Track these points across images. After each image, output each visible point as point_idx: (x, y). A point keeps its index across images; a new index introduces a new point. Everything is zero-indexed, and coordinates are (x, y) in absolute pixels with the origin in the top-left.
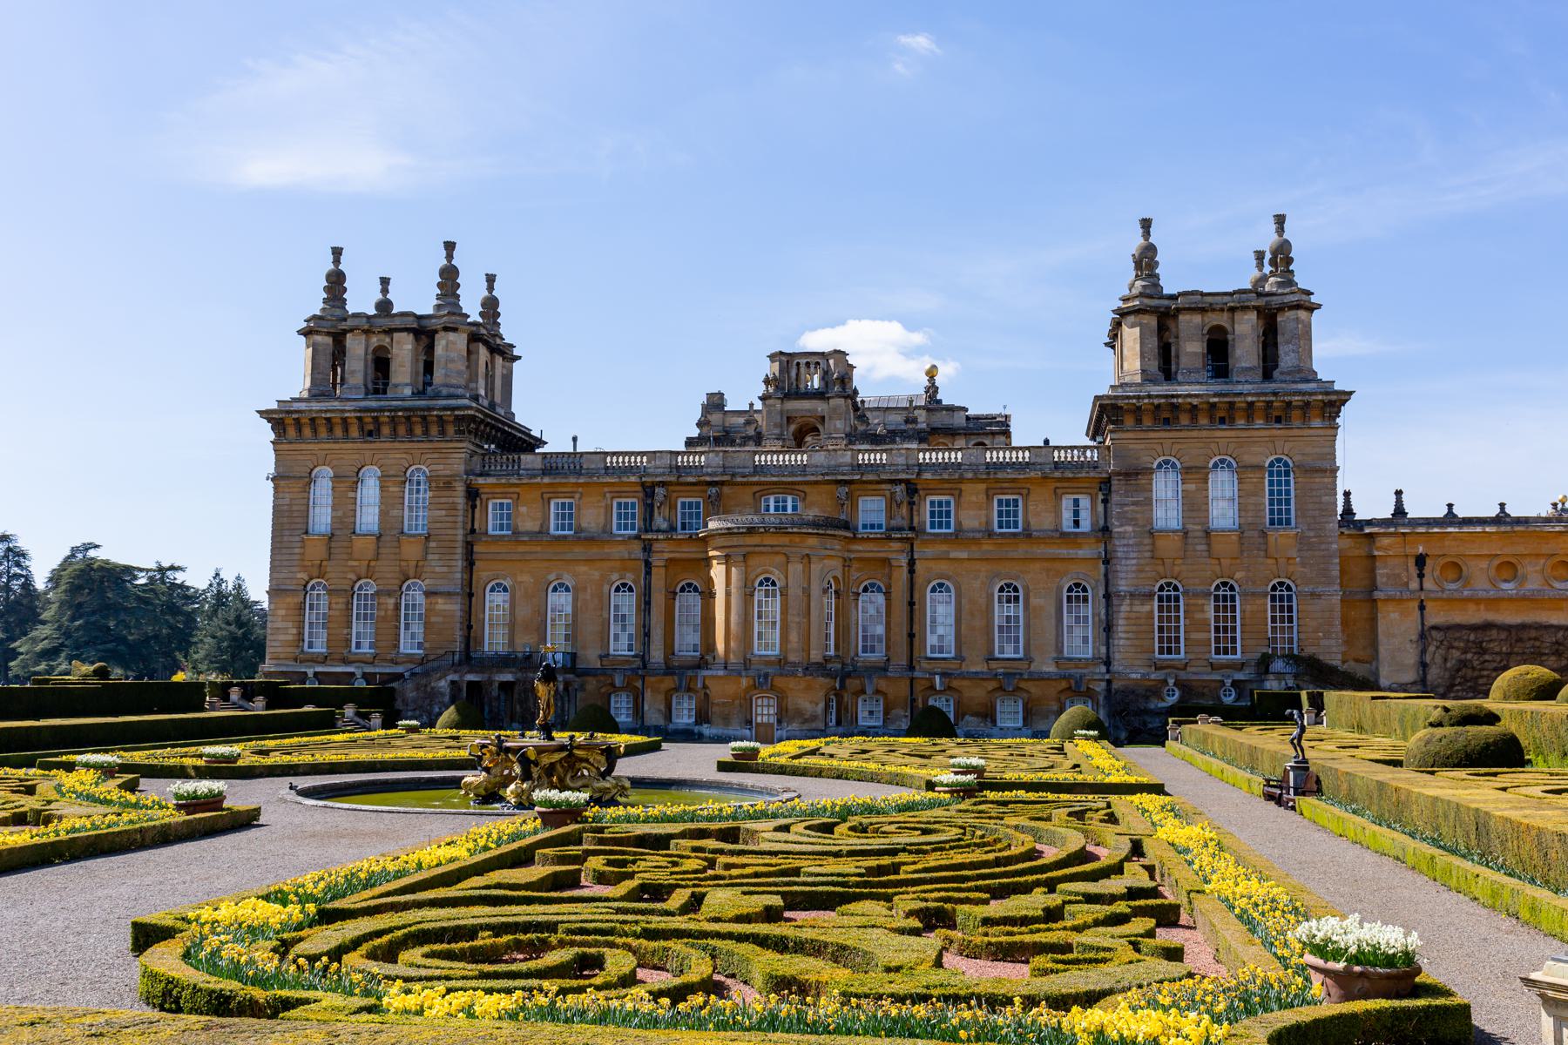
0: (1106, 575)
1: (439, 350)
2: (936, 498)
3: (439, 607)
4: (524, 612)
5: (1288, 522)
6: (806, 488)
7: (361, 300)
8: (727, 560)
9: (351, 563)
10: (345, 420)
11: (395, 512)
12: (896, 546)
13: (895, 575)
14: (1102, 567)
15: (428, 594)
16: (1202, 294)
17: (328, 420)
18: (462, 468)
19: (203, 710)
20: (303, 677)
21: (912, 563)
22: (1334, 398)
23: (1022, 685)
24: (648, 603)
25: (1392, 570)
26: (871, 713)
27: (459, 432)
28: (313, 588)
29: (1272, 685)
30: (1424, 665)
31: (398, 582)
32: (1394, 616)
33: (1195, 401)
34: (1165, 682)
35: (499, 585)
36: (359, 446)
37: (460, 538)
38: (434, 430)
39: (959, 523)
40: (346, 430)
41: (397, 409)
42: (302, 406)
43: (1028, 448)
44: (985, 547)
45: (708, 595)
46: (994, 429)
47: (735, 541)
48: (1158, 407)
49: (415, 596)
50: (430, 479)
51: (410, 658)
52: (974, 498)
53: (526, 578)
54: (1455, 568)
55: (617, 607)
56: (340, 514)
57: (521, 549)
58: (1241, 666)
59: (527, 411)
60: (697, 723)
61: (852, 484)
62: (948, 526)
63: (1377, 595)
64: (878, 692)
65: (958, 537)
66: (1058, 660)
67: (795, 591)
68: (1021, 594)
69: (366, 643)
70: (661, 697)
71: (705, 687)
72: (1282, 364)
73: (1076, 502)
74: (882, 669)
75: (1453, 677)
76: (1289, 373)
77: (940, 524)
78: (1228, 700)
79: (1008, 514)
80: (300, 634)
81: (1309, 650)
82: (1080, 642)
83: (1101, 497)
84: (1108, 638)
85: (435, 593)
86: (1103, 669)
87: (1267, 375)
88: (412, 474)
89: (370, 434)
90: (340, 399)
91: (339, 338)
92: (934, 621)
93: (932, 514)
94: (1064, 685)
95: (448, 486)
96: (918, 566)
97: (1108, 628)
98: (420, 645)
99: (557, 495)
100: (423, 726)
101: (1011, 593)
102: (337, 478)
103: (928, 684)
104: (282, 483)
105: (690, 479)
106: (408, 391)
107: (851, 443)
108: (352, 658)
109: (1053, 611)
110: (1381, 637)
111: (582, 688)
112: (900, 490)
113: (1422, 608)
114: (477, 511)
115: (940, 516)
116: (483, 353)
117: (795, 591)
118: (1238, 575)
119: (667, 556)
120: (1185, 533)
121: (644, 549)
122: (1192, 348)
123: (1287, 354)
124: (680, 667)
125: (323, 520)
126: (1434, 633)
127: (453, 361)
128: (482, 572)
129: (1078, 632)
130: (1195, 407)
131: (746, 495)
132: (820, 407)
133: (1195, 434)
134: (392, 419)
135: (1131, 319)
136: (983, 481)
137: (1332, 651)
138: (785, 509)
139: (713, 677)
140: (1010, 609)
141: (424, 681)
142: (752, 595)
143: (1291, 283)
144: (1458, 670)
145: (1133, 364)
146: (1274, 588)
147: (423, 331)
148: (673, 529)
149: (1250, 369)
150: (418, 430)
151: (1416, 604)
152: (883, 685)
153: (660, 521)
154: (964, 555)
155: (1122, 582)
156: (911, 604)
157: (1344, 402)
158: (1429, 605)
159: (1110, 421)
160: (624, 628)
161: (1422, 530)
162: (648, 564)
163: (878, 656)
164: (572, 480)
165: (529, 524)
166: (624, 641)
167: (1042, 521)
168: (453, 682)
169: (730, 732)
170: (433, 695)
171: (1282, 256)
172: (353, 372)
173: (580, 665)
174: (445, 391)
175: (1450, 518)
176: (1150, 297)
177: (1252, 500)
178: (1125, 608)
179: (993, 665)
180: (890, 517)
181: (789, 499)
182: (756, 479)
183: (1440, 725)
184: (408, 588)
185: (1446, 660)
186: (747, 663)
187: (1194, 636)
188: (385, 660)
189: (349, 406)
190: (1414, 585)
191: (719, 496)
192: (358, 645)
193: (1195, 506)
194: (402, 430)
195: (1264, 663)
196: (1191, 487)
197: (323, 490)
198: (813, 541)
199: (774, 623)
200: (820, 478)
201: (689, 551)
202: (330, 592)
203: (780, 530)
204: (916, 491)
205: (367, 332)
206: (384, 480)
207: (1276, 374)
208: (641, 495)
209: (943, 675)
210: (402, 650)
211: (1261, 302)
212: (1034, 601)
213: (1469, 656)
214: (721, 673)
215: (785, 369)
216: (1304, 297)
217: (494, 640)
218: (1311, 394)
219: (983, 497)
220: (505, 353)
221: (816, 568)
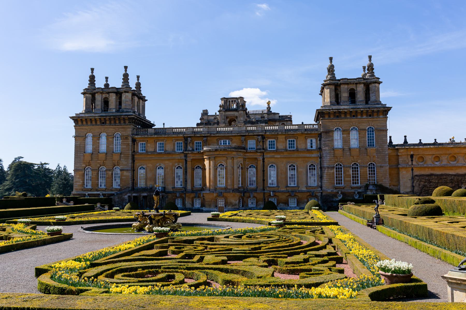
0: (320, 162)
1: (123, 98)
2: (270, 140)
3: (124, 174)
4: (149, 175)
5: (373, 145)
6: (232, 138)
7: (100, 84)
8: (209, 159)
10: (95, 119)
11: (111, 146)
12: (259, 154)
13: (259, 162)
14: (319, 160)
15: (121, 170)
16: (348, 79)
17: (91, 119)
18: (131, 133)
19: (55, 205)
20: (85, 195)
21: (263, 159)
22: (386, 109)
23: (296, 194)
24: (186, 172)
25: (404, 158)
26: (252, 203)
27: (129, 122)
28: (87, 169)
29: (369, 193)
30: (413, 187)
31: (112, 167)
32: (404, 172)
33: (346, 111)
34: (338, 193)
35: (142, 167)
37: (130, 154)
38: (122, 122)
39: (277, 147)
41: (111, 116)
42: (83, 115)
43: (297, 125)
44: (285, 154)
45: (204, 169)
46: (287, 119)
47: (211, 153)
48: (335, 112)
49: (117, 171)
50: (121, 136)
51: (116, 189)
52: (281, 140)
54: (422, 158)
55: (177, 173)
56: (94, 147)
58: (360, 188)
59: (150, 116)
60: (201, 207)
61: (246, 136)
62: (274, 148)
63: (399, 166)
64: (254, 197)
65: (277, 151)
66: (307, 187)
67: (229, 168)
68: (296, 168)
69: (103, 185)
70: (190, 200)
71: (203, 196)
72: (371, 99)
73: (311, 141)
74: (255, 190)
75: (421, 190)
76: (373, 102)
77: (272, 147)
78: (357, 197)
79: (292, 144)
80: (84, 183)
81: (380, 183)
82: (313, 181)
83: (319, 139)
84: (321, 180)
85: (123, 170)
86: (320, 189)
87: (367, 103)
88: (116, 135)
89: (103, 123)
90: (94, 113)
91: (93, 95)
92: (270, 176)
93: (269, 145)
94: (308, 194)
95: (126, 138)
96: (266, 160)
97: (321, 177)
98: (119, 185)
99: (159, 140)
100: (121, 209)
101: (293, 167)
102: (93, 136)
103: (269, 194)
104: (77, 138)
105: (198, 135)
106: (114, 111)
107: (245, 124)
108: (99, 189)
109: (305, 172)
110: (401, 179)
111: (167, 197)
112: (260, 138)
113: (412, 170)
114: (135, 146)
115: (272, 145)
116: (136, 99)
117: (229, 168)
118: (359, 161)
119: (191, 158)
120: (343, 149)
121: (185, 156)
122: (345, 95)
123: (372, 96)
124: (196, 191)
125: (90, 149)
126: (416, 177)
127: (127, 101)
128: (137, 163)
129: (312, 178)
130: (346, 112)
131: (215, 140)
132: (236, 113)
133: (346, 120)
134: (110, 119)
135: (327, 87)
136: (284, 135)
137: (386, 183)
138: (226, 144)
139: (206, 193)
140: (293, 172)
141: (120, 196)
142: (217, 169)
143: (373, 76)
144: (423, 188)
145: (328, 100)
146: (369, 165)
147: (118, 92)
148: (193, 150)
149: (362, 101)
150: (117, 122)
151: (411, 169)
152: (255, 195)
153: (189, 148)
154: (279, 156)
155: (325, 164)
156: (264, 171)
157: (389, 110)
158: (414, 169)
159: (321, 117)
160: (179, 179)
161: (412, 147)
162: (186, 161)
163: (254, 186)
164: (163, 136)
165: (151, 149)
166: (179, 183)
167: (301, 146)
168: (129, 196)
169: (211, 209)
170: (123, 200)
171: (371, 68)
172: (98, 105)
173: (167, 190)
174: (125, 110)
175: (420, 144)
176: (332, 80)
177: (363, 139)
178: (326, 171)
179: (288, 188)
180: (257, 146)
181: (227, 141)
182: (217, 135)
183: (418, 204)
184: (115, 169)
185: (419, 185)
186: (215, 189)
187: (346, 179)
188: (109, 190)
189: (97, 115)
190: (410, 163)
191: (207, 140)
192: (101, 186)
193: (346, 141)
194: (112, 122)
195: (367, 187)
196: (345, 136)
197: (89, 140)
198: (234, 153)
199: (223, 177)
200: (236, 134)
201: (198, 157)
202: (92, 170)
203: (225, 150)
204: (265, 138)
205: (102, 93)
206: (107, 137)
207: (369, 102)
209: (273, 192)
210: (114, 187)
211: (365, 81)
212: (299, 170)
213: (426, 184)
214: (208, 192)
215: (225, 102)
216: (377, 80)
217: (141, 184)
218: (379, 108)
219: (284, 139)
220: (143, 99)
221: (235, 161)
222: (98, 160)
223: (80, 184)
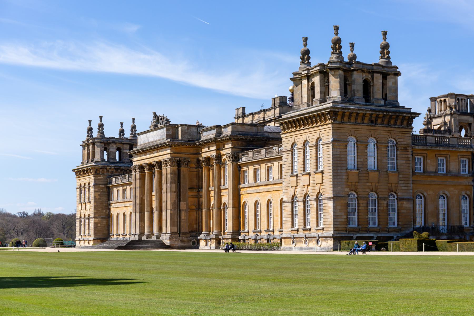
3: (405, 205)
7: (346, 54)
9: (368, 184)
15: (399, 199)
36: (369, 127)
40: (363, 119)
53: (431, 192)
57: (429, 179)
89: (372, 122)
134: (384, 116)
150: (392, 122)
172: (358, 91)
188: (384, 230)
197: (351, 148)
206: (378, 145)
208: (470, 157)
222: (368, 181)
223: (343, 220)
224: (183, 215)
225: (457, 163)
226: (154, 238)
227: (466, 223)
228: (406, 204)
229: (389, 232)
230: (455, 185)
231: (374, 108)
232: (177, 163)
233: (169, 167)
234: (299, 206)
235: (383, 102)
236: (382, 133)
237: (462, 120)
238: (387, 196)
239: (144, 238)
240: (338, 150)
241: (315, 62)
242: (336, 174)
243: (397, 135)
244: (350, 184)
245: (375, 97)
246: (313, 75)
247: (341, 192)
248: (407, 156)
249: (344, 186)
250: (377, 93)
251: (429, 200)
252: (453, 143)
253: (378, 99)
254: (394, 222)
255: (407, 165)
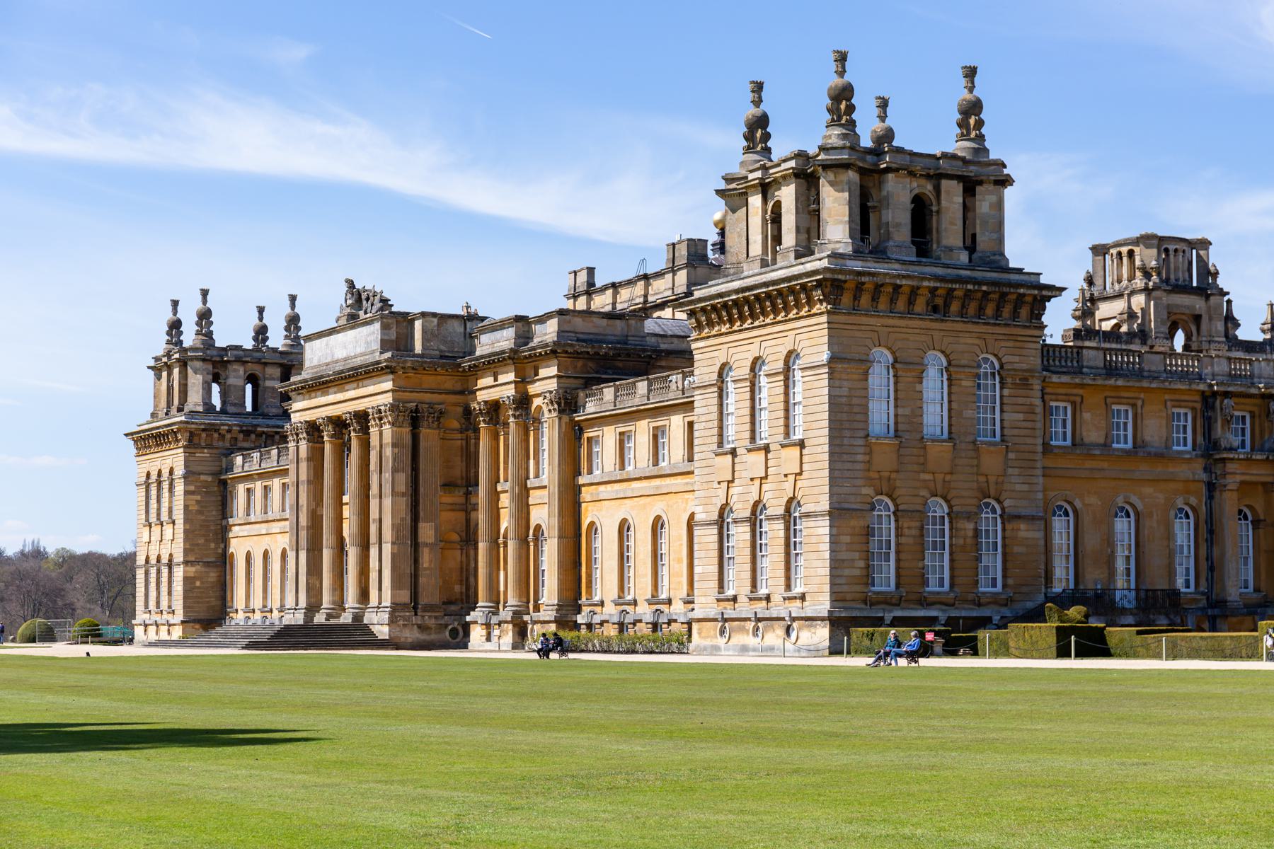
3: (1022, 534)
15: (1007, 518)
40: (911, 302)
53: (1093, 500)
57: (1089, 464)
89: (935, 309)
108: (932, 598)
119: (1239, 478)
134: (968, 294)
150: (990, 310)
172: (898, 225)
188: (966, 601)
197: (880, 380)
206: (951, 371)
208: (1198, 406)
222: (923, 466)
223: (857, 572)
224: (426, 558)
225: (1164, 422)
226: (346, 618)
227: (1187, 581)
228: (1025, 532)
229: (979, 605)
230: (1158, 480)
231: (939, 271)
232: (412, 418)
233: (387, 429)
234: (740, 535)
235: (964, 257)
236: (962, 340)
237: (1178, 306)
238: (975, 510)
239: (320, 618)
240: (845, 383)
241: (782, 146)
242: (837, 449)
243: (1003, 344)
244: (876, 476)
245: (945, 242)
246: (777, 183)
247: (852, 499)
248: (1028, 401)
249: (859, 482)
250: (949, 231)
251: (1086, 519)
252: (1153, 368)
253: (951, 249)
254: (994, 580)
255: (1029, 425)
